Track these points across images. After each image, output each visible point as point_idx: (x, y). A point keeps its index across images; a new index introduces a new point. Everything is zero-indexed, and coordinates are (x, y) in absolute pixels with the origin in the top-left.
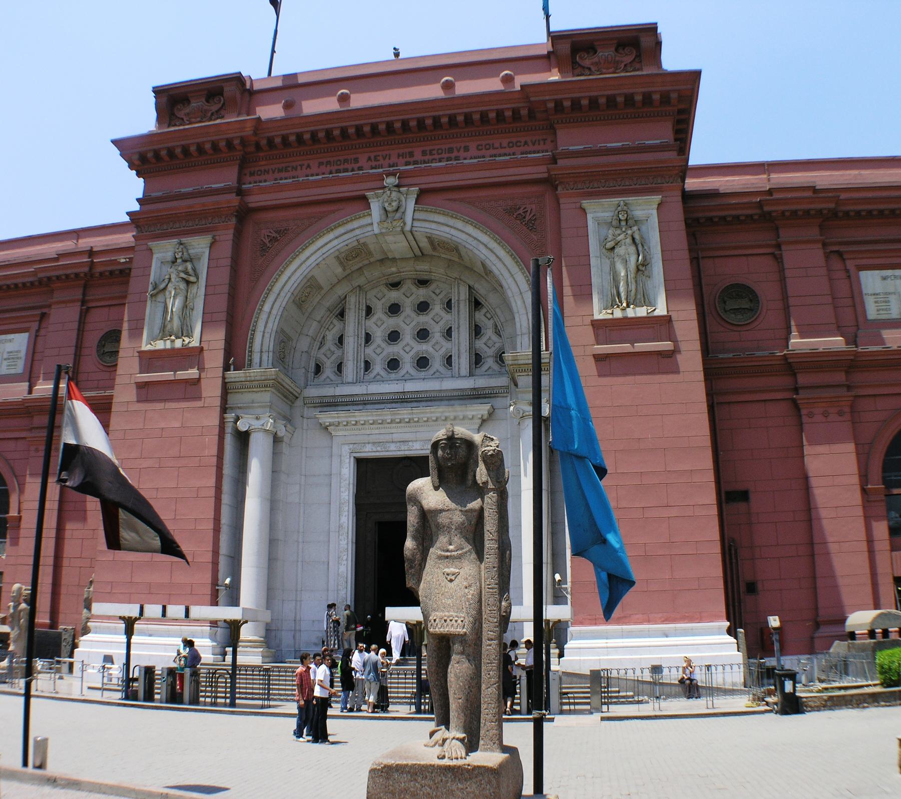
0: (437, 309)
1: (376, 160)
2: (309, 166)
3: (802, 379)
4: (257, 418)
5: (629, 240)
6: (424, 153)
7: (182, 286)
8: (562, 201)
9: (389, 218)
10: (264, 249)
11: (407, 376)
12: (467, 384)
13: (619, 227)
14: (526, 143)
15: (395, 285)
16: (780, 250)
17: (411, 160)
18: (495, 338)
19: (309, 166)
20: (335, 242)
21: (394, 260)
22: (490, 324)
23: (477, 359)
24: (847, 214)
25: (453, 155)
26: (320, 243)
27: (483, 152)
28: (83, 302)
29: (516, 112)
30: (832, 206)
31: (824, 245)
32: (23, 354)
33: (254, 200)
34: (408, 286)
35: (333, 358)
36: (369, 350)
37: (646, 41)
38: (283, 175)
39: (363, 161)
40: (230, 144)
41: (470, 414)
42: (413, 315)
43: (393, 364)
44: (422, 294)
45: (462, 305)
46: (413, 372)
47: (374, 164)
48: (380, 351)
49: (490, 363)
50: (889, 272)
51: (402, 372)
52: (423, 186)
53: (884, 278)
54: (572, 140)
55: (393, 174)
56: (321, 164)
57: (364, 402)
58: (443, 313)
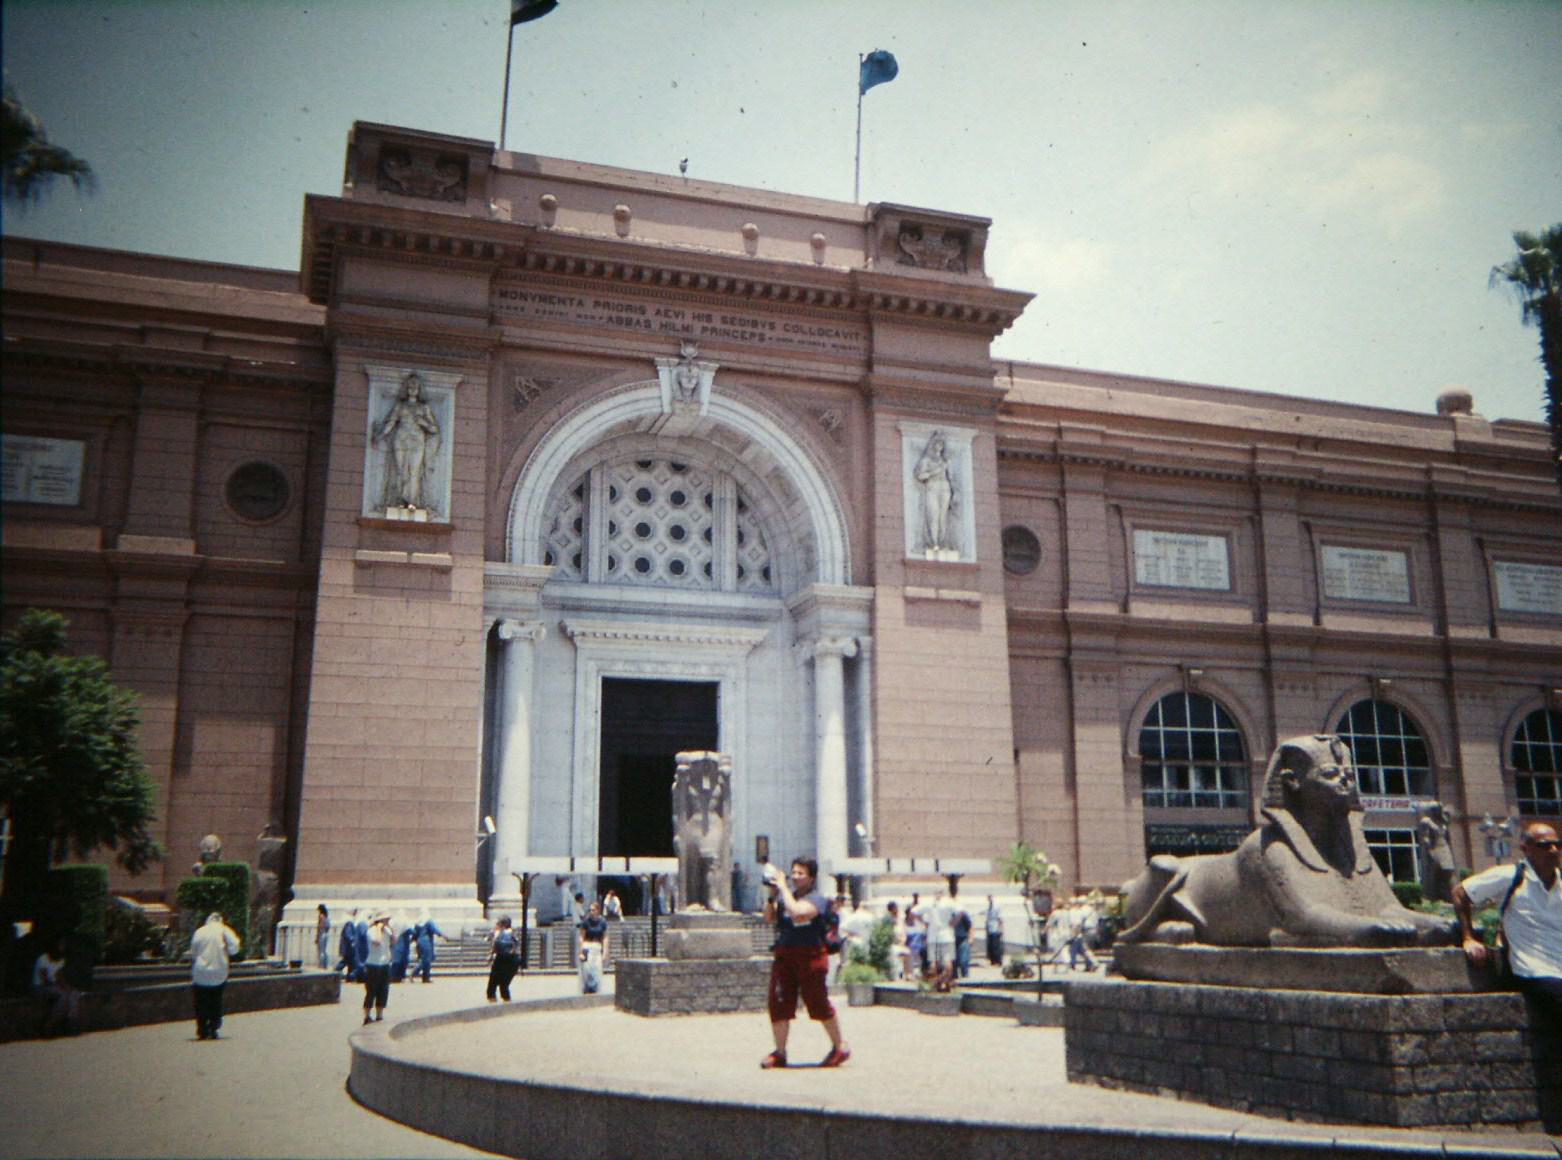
1: (666, 315)
2: (580, 303)
3: (1077, 640)
4: (522, 624)
6: (724, 320)
7: (421, 436)
9: (675, 391)
10: (518, 403)
11: (660, 582)
12: (738, 602)
13: (934, 459)
14: (837, 334)
15: (645, 465)
18: (760, 550)
19: (580, 303)
20: (611, 414)
22: (755, 531)
23: (741, 572)
24: (1133, 468)
25: (758, 330)
26: (596, 409)
27: (789, 335)
28: (202, 414)
30: (1122, 458)
31: (1106, 496)
32: (76, 473)
33: (514, 333)
34: (662, 469)
35: (571, 546)
36: (615, 545)
37: (976, 236)
38: (549, 307)
39: (650, 314)
40: (488, 251)
41: (743, 639)
42: (668, 507)
43: (643, 565)
44: (677, 482)
45: (728, 504)
46: (666, 577)
47: (664, 320)
48: (630, 547)
49: (754, 578)
50: (1161, 535)
51: (654, 576)
52: (725, 364)
54: (890, 342)
56: (597, 304)
57: (615, 610)
58: (702, 510)
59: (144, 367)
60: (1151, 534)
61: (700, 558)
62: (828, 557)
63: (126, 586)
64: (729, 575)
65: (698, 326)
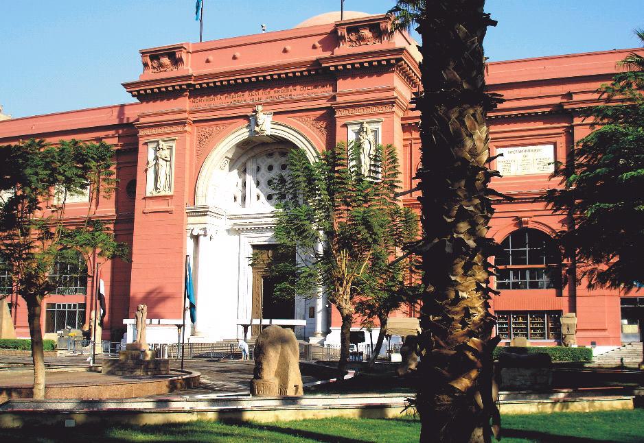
6: (275, 92)
15: (270, 155)
25: (290, 92)
34: (277, 156)
44: (283, 160)
54: (344, 85)
55: (260, 104)
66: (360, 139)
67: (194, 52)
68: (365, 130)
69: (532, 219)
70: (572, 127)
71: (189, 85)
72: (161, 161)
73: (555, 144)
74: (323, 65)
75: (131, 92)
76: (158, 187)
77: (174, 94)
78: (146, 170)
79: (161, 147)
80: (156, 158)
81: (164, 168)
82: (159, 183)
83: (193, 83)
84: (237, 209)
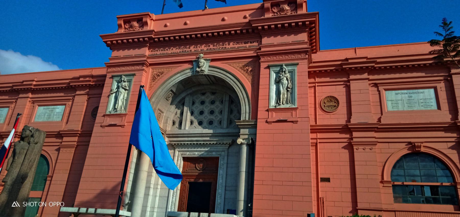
0: (217, 103)
5: (285, 78)
6: (214, 46)
8: (261, 64)
15: (203, 94)
16: (349, 83)
17: (209, 48)
20: (180, 77)
21: (203, 85)
25: (225, 46)
29: (247, 30)
34: (208, 94)
38: (163, 52)
44: (213, 97)
47: (195, 49)
50: (400, 91)
53: (397, 94)
55: (202, 53)
58: (220, 105)
59: (75, 85)
60: (394, 92)
61: (218, 119)
62: (244, 112)
63: (65, 139)
64: (225, 123)
65: (205, 49)
66: (280, 77)
67: (156, 20)
68: (284, 70)
69: (422, 145)
70: (450, 76)
71: (150, 38)
72: (121, 90)
73: (435, 89)
74: (253, 25)
75: (106, 42)
76: (116, 107)
77: (138, 44)
78: (109, 96)
79: (123, 79)
80: (118, 88)
81: (123, 94)
82: (117, 105)
83: (153, 37)
84: (176, 131)
